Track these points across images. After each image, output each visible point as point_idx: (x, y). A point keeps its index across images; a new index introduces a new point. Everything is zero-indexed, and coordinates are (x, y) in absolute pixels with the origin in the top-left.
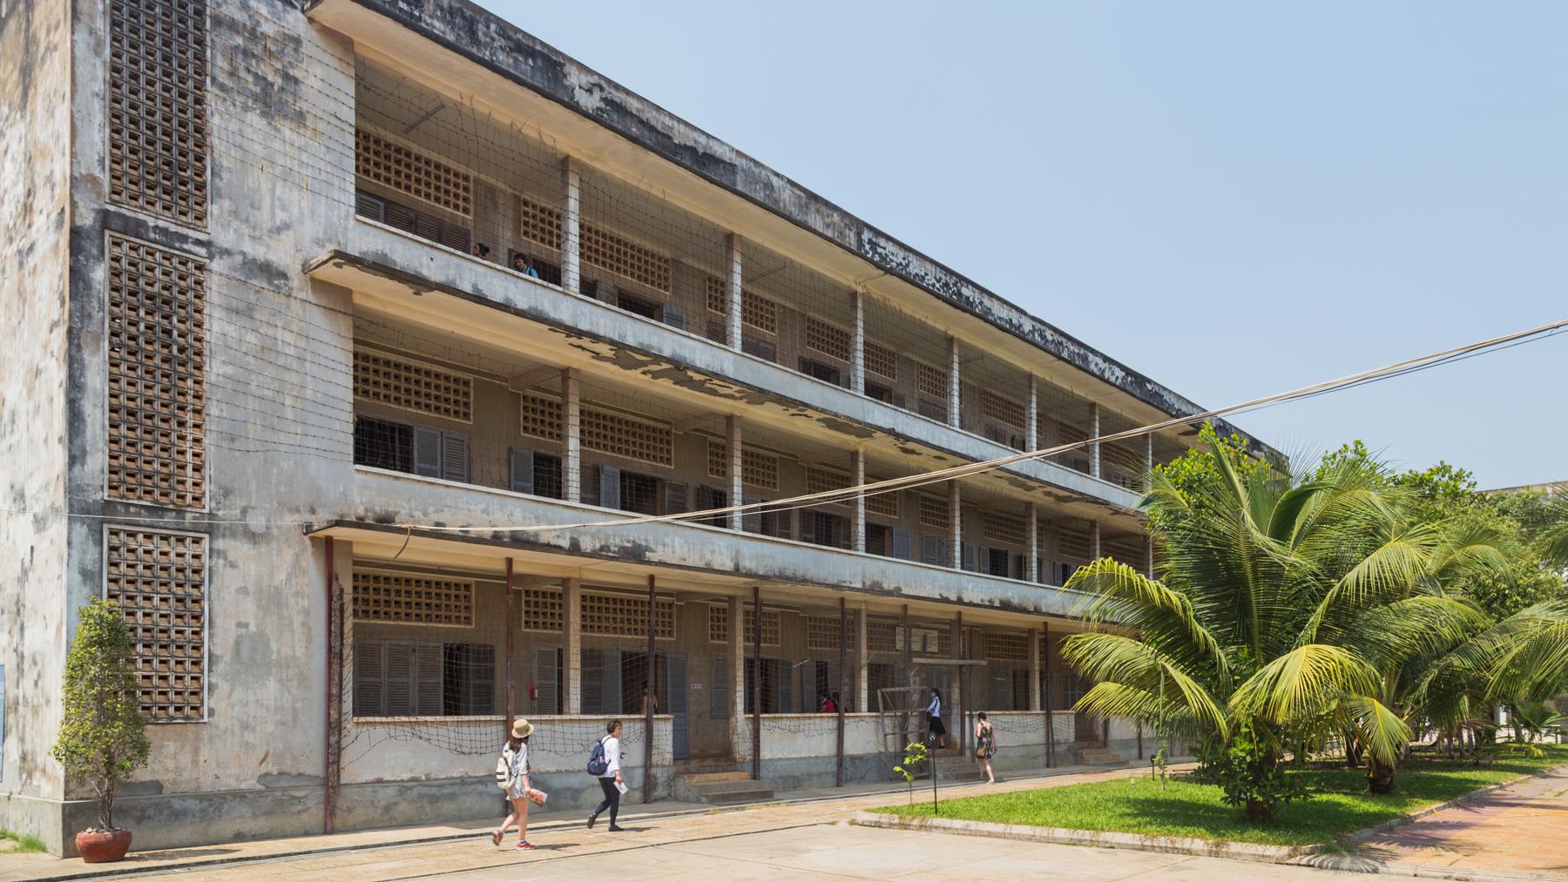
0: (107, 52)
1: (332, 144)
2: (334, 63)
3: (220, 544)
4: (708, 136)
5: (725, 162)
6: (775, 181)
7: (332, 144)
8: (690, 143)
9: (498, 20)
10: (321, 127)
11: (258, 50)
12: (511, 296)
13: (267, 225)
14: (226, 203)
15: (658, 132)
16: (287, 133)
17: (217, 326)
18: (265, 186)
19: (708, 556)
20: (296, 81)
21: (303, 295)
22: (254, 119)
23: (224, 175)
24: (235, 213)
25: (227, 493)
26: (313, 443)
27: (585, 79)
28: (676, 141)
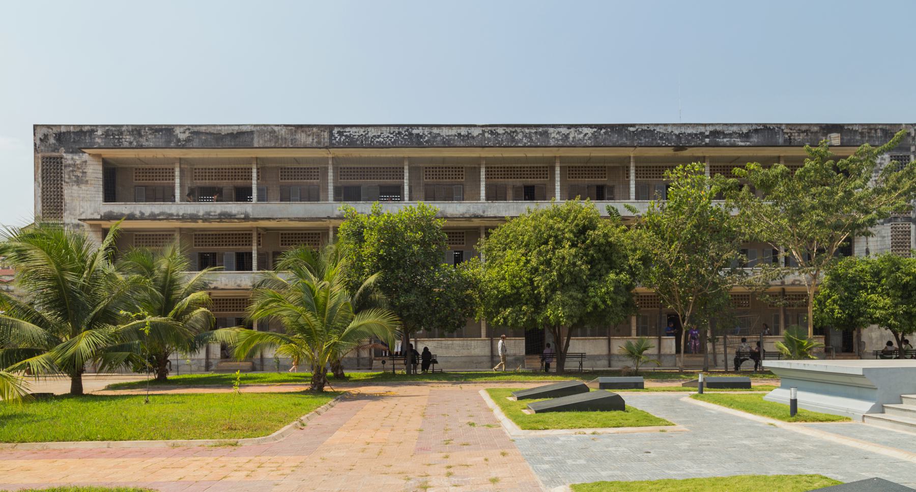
0: (41, 185)
1: (95, 186)
2: (96, 163)
4: (239, 125)
5: (248, 132)
6: (276, 129)
7: (95, 186)
8: (229, 132)
9: (148, 126)
10: (93, 182)
12: (153, 210)
13: (79, 214)
15: (214, 134)
18: (77, 203)
20: (86, 173)
21: (88, 229)
22: (75, 187)
23: (68, 205)
27: (182, 129)
28: (223, 134)
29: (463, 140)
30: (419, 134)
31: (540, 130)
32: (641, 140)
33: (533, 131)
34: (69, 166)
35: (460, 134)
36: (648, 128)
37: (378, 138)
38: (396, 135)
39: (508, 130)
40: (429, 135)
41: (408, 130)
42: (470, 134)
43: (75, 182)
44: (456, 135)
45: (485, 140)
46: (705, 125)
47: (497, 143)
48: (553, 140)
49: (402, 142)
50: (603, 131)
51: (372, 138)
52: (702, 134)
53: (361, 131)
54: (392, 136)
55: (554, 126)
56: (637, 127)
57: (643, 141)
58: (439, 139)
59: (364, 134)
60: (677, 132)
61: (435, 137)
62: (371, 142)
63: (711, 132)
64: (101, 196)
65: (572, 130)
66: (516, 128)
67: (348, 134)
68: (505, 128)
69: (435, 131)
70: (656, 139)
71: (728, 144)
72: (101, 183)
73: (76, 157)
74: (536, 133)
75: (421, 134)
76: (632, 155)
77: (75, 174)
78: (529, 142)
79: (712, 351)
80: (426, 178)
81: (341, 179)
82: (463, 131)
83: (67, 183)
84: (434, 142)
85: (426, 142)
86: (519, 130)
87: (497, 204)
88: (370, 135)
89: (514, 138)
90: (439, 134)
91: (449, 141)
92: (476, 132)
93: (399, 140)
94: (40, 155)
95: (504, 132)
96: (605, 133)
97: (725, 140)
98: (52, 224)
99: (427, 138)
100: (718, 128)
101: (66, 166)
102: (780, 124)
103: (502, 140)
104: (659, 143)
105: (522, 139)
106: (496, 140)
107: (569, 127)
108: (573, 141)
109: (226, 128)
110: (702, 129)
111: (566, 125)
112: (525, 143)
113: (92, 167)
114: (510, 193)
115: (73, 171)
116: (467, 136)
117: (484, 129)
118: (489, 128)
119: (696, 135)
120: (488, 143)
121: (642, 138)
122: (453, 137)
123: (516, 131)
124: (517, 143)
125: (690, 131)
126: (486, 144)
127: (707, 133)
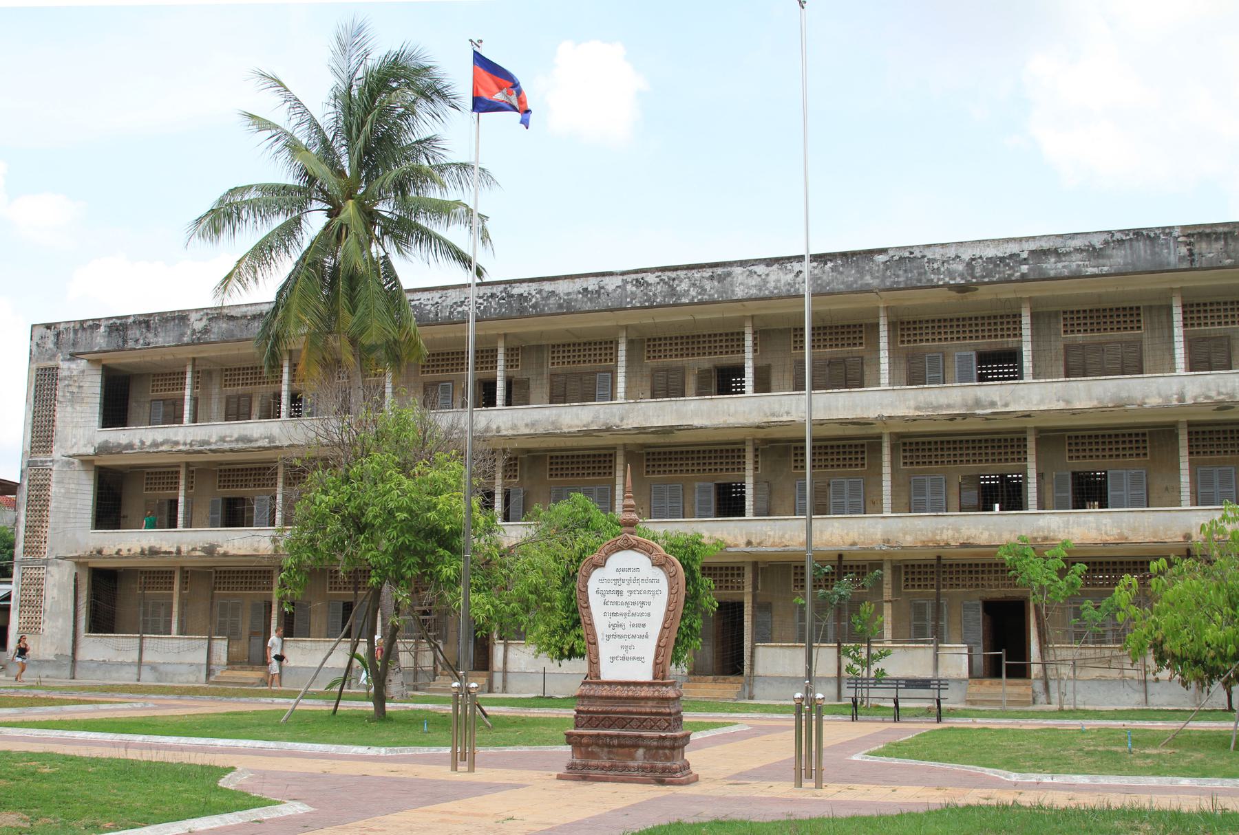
3: (49, 568)
9: (160, 314)
11: (71, 383)
14: (58, 444)
16: (78, 408)
17: (54, 489)
19: (256, 545)
22: (69, 409)
24: (61, 446)
25: (52, 549)
26: (78, 525)
27: (198, 316)
29: (590, 300)
30: (522, 295)
31: (719, 271)
32: (898, 276)
33: (707, 273)
34: (65, 378)
35: (586, 290)
36: (912, 253)
37: (461, 306)
38: (487, 300)
39: (665, 276)
40: (538, 296)
41: (505, 289)
42: (603, 288)
43: (70, 401)
44: (579, 293)
45: (626, 297)
46: (1020, 240)
47: (646, 301)
48: (741, 287)
49: (495, 309)
50: (830, 265)
51: (452, 306)
52: (1012, 256)
53: (436, 296)
54: (481, 301)
55: (743, 263)
56: (891, 253)
57: (901, 279)
58: (552, 300)
59: (440, 301)
60: (966, 256)
61: (548, 298)
62: (451, 313)
63: (1032, 252)
64: (97, 419)
65: (776, 266)
66: (679, 272)
67: (417, 302)
68: (660, 274)
69: (548, 287)
70: (925, 273)
71: (1066, 272)
72: (98, 400)
73: (73, 366)
74: (712, 278)
75: (525, 294)
76: (882, 305)
77: (71, 389)
78: (700, 294)
79: (1042, 674)
80: (553, 364)
81: (423, 372)
82: (592, 284)
83: (61, 402)
84: (544, 306)
85: (534, 306)
86: (681, 274)
87: (643, 405)
88: (449, 302)
89: (674, 289)
90: (553, 292)
91: (569, 302)
92: (611, 284)
93: (491, 307)
94: (34, 366)
95: (658, 280)
96: (832, 269)
97: (1060, 265)
98: (41, 462)
99: (534, 300)
100: (1045, 245)
101: (61, 380)
102: (1169, 228)
103: (655, 295)
104: (932, 280)
105: (689, 290)
106: (646, 294)
107: (769, 262)
108: (776, 288)
109: (253, 308)
110: (1014, 248)
111: (765, 259)
112: (693, 297)
113: (89, 379)
114: (691, 383)
115: (68, 386)
116: (598, 292)
117: (625, 277)
118: (634, 276)
119: (1002, 259)
120: (631, 302)
121: (901, 272)
122: (575, 297)
123: (678, 277)
124: (679, 298)
125: (990, 252)
126: (628, 303)
127: (1025, 255)
